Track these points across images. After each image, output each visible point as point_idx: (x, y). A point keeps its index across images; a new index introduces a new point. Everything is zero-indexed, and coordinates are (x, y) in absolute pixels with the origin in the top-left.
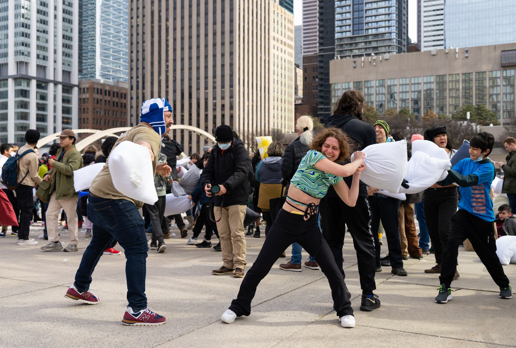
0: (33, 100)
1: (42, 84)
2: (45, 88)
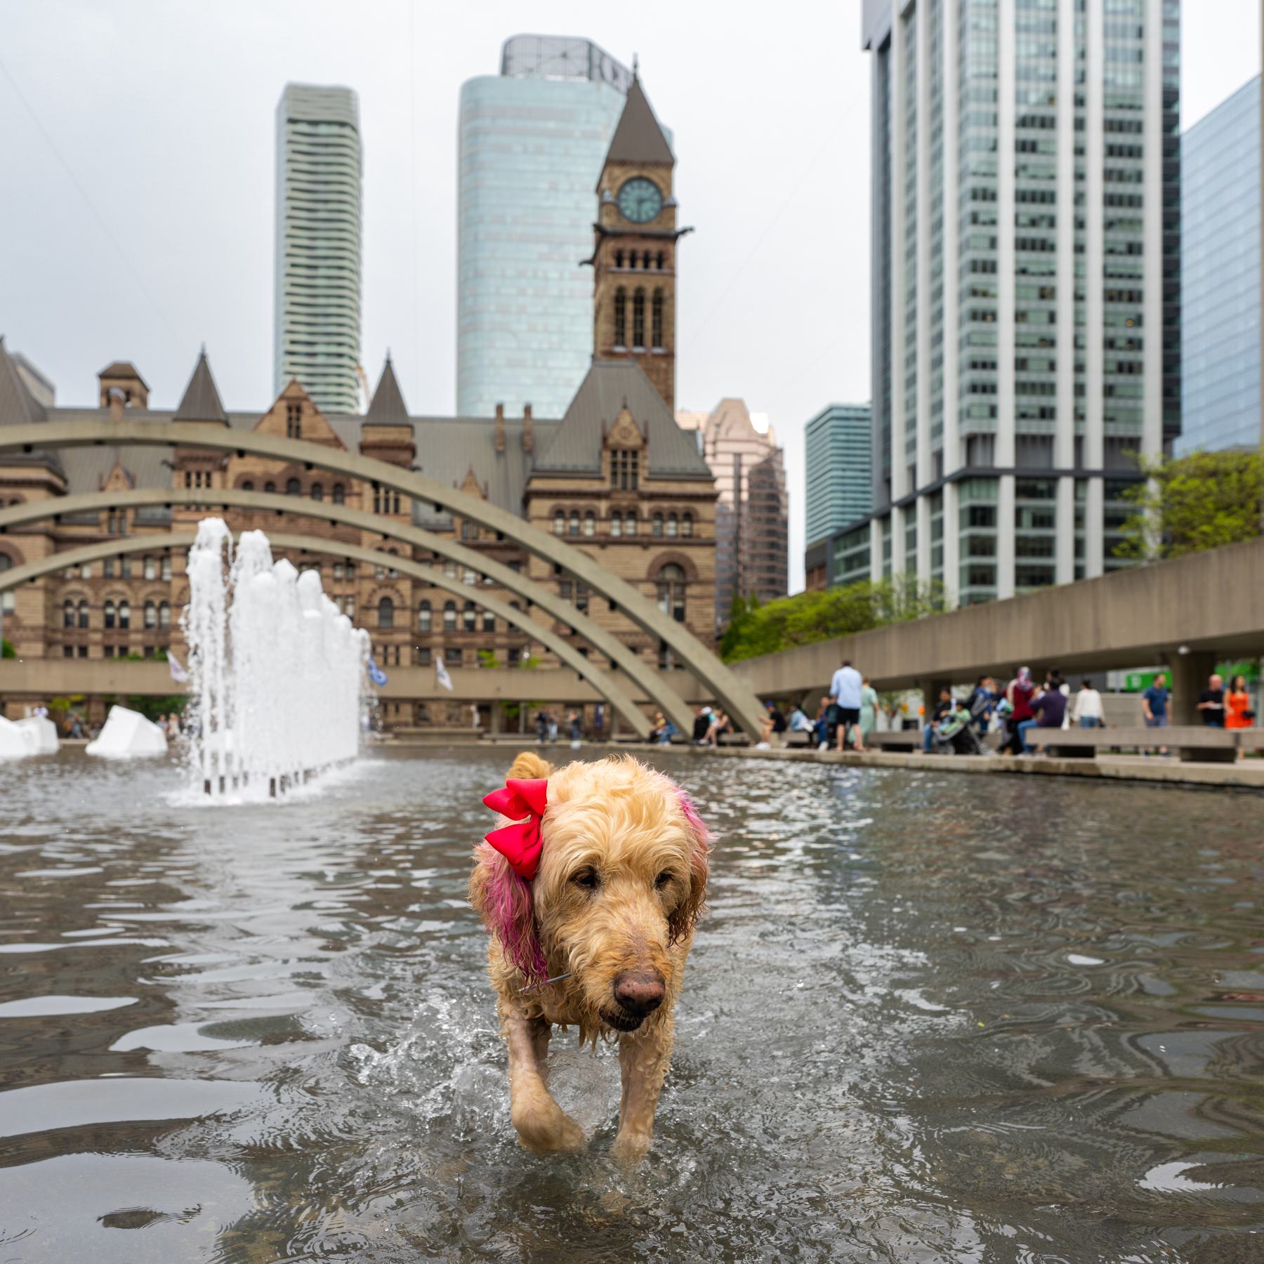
0: (1005, 532)
1: (1035, 486)
2: (1051, 493)
